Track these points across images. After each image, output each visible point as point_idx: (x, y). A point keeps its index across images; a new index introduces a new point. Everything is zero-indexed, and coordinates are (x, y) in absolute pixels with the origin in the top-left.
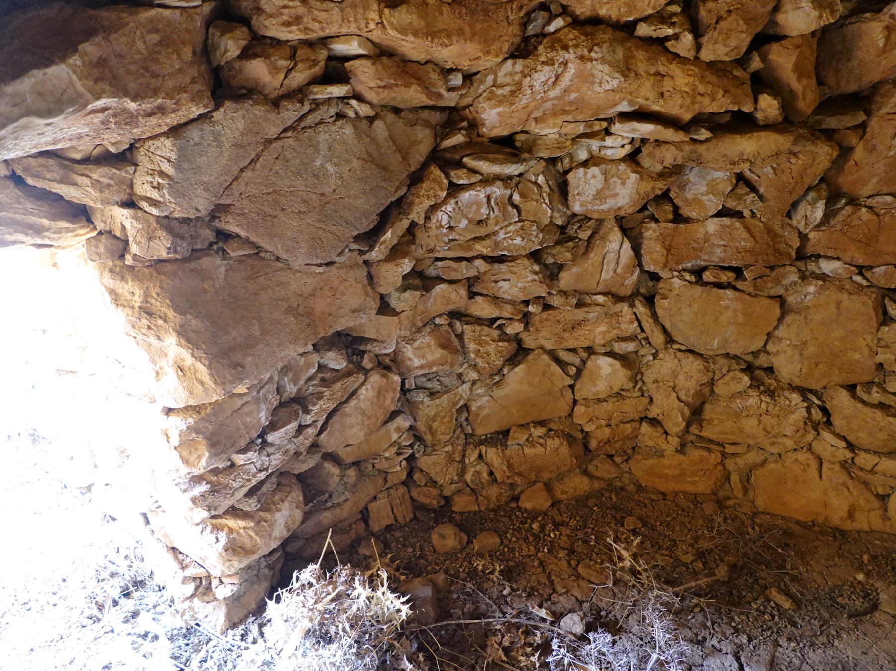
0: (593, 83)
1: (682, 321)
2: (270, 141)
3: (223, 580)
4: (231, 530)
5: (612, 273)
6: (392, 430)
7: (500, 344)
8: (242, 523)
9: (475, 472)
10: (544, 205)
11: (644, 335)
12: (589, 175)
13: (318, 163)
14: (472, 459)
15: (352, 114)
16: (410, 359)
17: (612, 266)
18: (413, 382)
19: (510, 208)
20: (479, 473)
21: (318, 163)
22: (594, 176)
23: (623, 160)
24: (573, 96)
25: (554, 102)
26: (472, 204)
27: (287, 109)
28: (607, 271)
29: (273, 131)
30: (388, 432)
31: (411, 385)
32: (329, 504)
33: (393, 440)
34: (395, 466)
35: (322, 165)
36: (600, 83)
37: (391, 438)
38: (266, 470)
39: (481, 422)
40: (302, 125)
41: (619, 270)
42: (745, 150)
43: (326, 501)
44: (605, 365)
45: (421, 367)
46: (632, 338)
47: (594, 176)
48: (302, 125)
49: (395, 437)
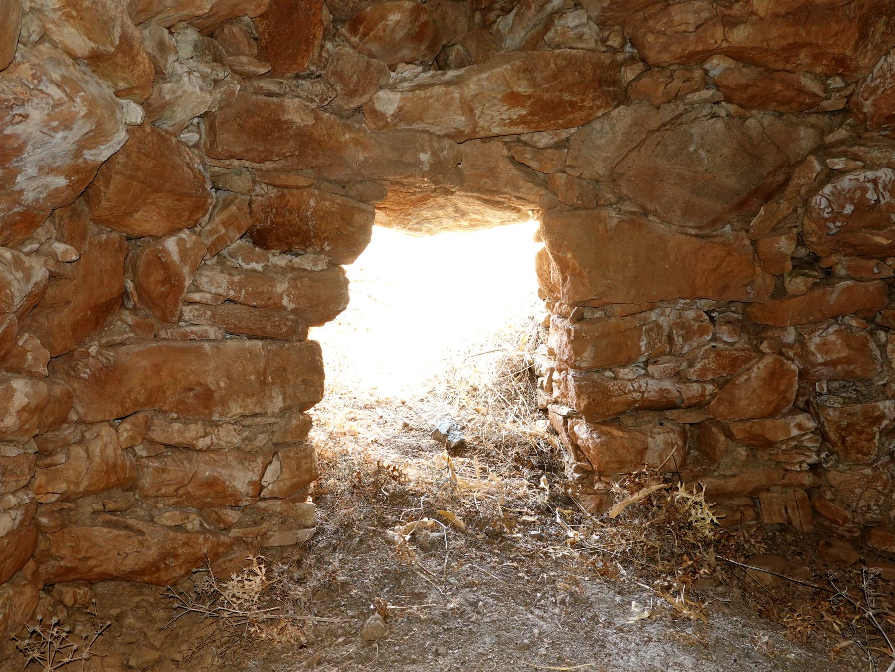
2: (652, 132)
4: (613, 437)
6: (792, 425)
8: (620, 434)
13: (691, 149)
15: (723, 113)
16: (813, 354)
18: (825, 386)
21: (691, 149)
26: (855, 191)
27: (666, 110)
29: (654, 125)
31: (822, 389)
32: (716, 473)
33: (792, 435)
34: (794, 464)
35: (695, 151)
37: (789, 432)
38: (643, 393)
40: (679, 121)
43: (715, 470)
45: (825, 364)
48: (679, 121)
49: (795, 432)
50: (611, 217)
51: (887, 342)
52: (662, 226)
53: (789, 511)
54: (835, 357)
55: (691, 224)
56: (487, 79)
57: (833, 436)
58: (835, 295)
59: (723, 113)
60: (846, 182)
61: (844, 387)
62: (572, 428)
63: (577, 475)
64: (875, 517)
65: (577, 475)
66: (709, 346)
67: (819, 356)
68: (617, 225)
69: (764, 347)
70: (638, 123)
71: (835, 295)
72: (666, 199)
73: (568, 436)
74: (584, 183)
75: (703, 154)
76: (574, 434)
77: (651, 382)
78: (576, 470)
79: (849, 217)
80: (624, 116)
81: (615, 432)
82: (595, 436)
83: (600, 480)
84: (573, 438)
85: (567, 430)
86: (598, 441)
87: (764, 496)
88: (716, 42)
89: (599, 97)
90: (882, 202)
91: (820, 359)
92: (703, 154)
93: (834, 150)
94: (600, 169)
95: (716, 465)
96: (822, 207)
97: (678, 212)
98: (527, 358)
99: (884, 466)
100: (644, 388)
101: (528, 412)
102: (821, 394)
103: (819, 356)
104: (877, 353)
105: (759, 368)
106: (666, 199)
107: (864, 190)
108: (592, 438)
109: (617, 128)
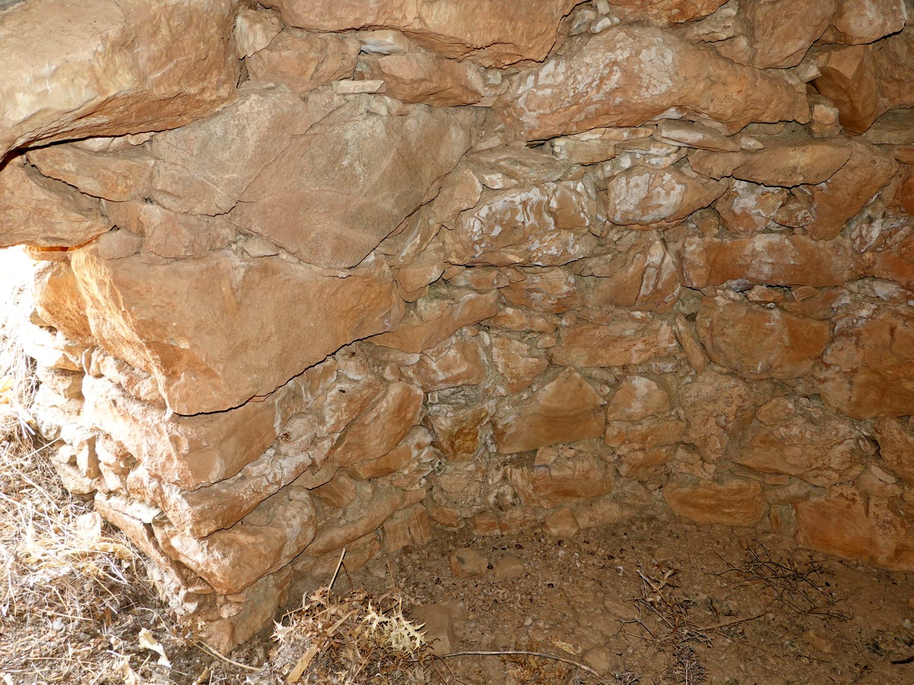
0: (640, 87)
1: (725, 342)
3: (229, 598)
4: (242, 548)
5: (651, 288)
7: (531, 360)
8: (251, 539)
9: (498, 493)
10: (582, 215)
11: (683, 355)
12: (632, 184)
13: (345, 163)
14: (496, 480)
16: (434, 372)
17: (652, 282)
19: (546, 216)
20: (503, 495)
21: (345, 163)
22: (637, 186)
23: (667, 169)
24: (618, 100)
25: (598, 106)
26: (506, 212)
28: (647, 287)
30: (408, 448)
32: (343, 522)
35: (351, 165)
36: (648, 88)
37: (410, 454)
38: (278, 483)
39: (507, 440)
41: (660, 286)
42: (798, 163)
43: (340, 518)
44: (641, 384)
45: (445, 381)
46: (670, 356)
47: (637, 186)
50: (235, 268)
51: (491, 345)
52: (302, 268)
53: (412, 531)
54: (455, 372)
55: (343, 265)
56: (54, 75)
57: (445, 445)
58: (459, 311)
59: (383, 111)
60: (499, 204)
61: (453, 393)
62: (167, 540)
63: (192, 607)
64: (479, 507)
65: (192, 607)
66: (334, 392)
67: (440, 373)
68: (244, 277)
69: (388, 374)
70: (279, 125)
71: (459, 311)
72: (313, 235)
73: (163, 553)
74: (193, 220)
75: (359, 169)
76: (171, 548)
77: (285, 463)
78: (188, 598)
79: (496, 239)
80: (258, 113)
81: (242, 538)
82: (217, 554)
83: (227, 601)
84: (171, 553)
85: (156, 544)
86: (226, 562)
87: (389, 525)
88: (405, 17)
89: (224, 82)
90: (527, 225)
91: (441, 376)
92: (359, 169)
93: (483, 159)
94: (221, 199)
95: (341, 512)
96: (475, 230)
97: (328, 252)
98: (25, 417)
99: (482, 457)
100: (279, 477)
101: (54, 506)
102: (431, 404)
103: (440, 373)
104: (484, 357)
105: (388, 402)
106: (313, 235)
107: (514, 211)
108: (216, 561)
109: (248, 133)
